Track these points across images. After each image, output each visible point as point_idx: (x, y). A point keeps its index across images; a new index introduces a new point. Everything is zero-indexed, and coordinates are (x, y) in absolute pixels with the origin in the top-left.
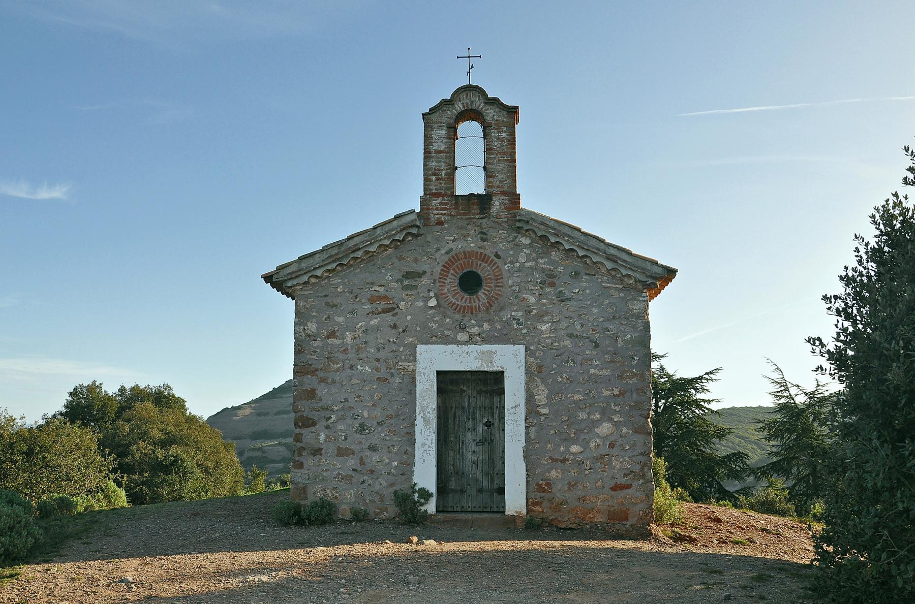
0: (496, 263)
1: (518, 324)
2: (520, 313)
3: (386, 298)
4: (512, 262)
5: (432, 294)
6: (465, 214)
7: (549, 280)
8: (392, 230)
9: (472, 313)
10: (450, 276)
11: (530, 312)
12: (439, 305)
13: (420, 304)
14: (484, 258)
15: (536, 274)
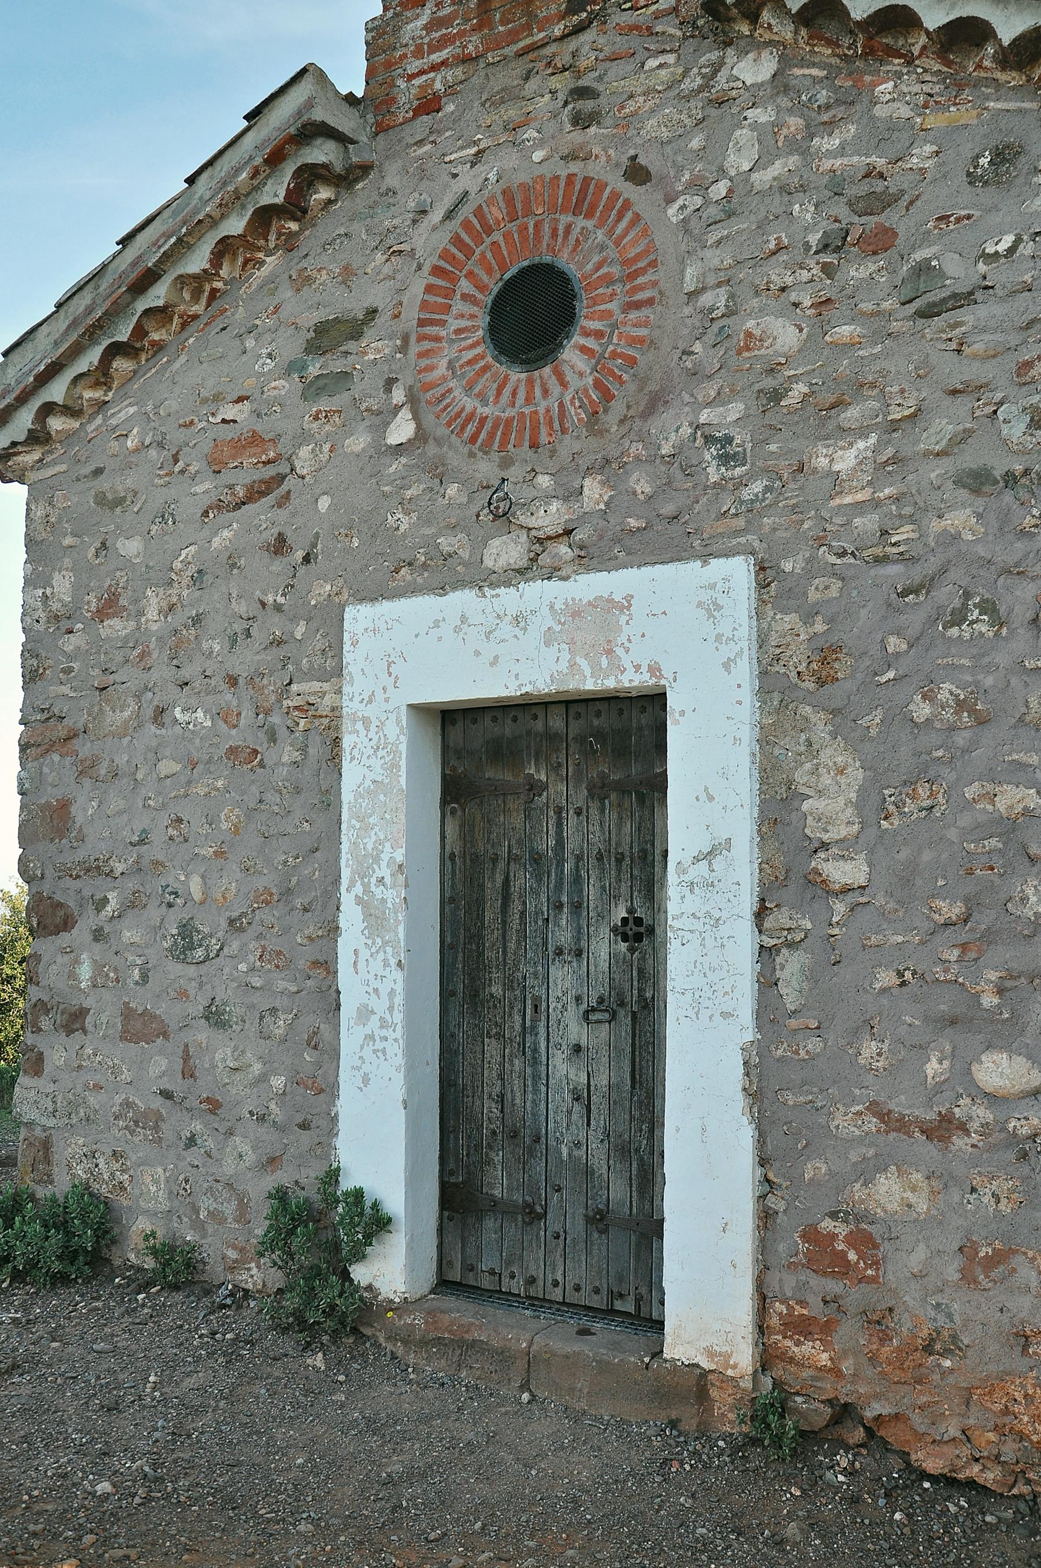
0: (627, 205)
1: (725, 459)
2: (735, 410)
3: (255, 440)
4: (699, 186)
5: (398, 395)
6: (513, 37)
7: (861, 225)
8: (237, 171)
9: (534, 445)
10: (459, 306)
11: (776, 396)
12: (421, 436)
13: (358, 442)
14: (583, 197)
15: (803, 211)
